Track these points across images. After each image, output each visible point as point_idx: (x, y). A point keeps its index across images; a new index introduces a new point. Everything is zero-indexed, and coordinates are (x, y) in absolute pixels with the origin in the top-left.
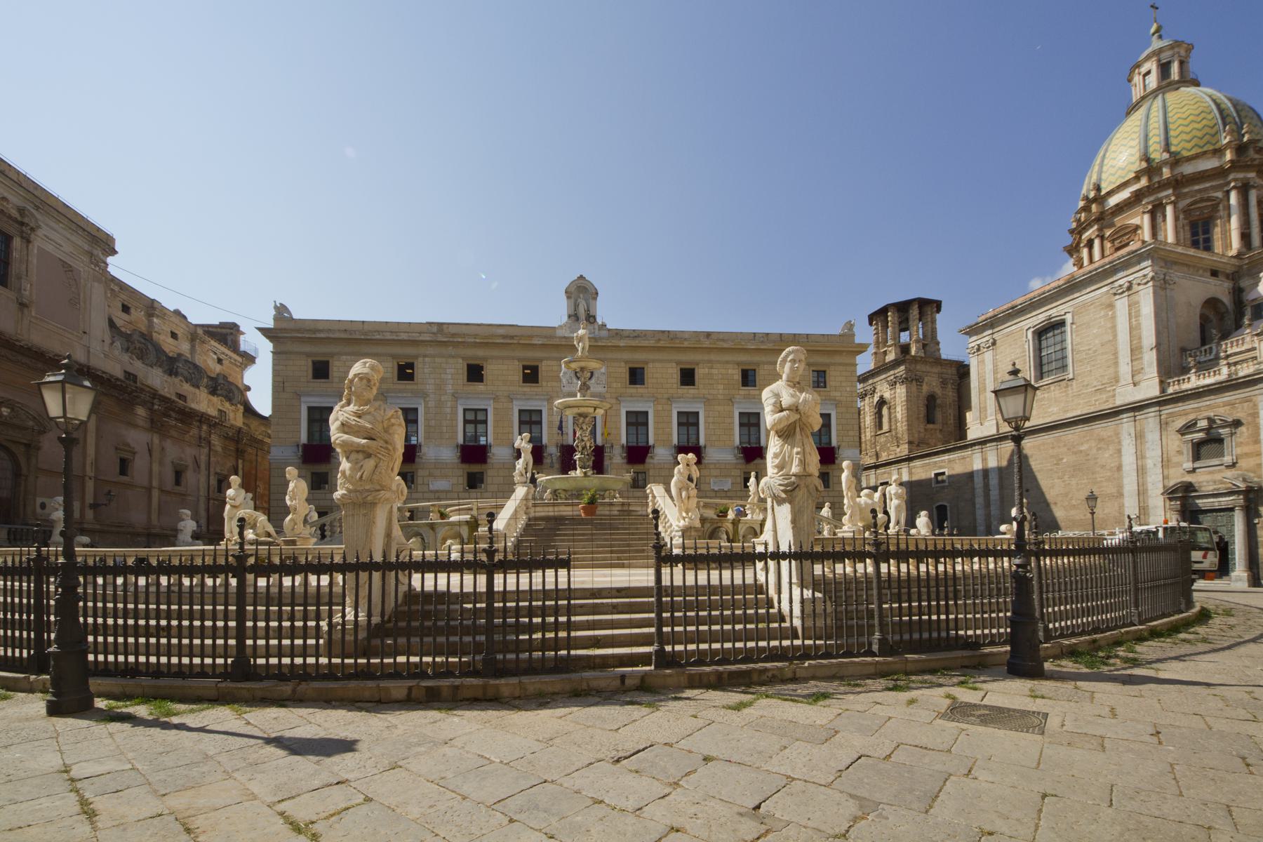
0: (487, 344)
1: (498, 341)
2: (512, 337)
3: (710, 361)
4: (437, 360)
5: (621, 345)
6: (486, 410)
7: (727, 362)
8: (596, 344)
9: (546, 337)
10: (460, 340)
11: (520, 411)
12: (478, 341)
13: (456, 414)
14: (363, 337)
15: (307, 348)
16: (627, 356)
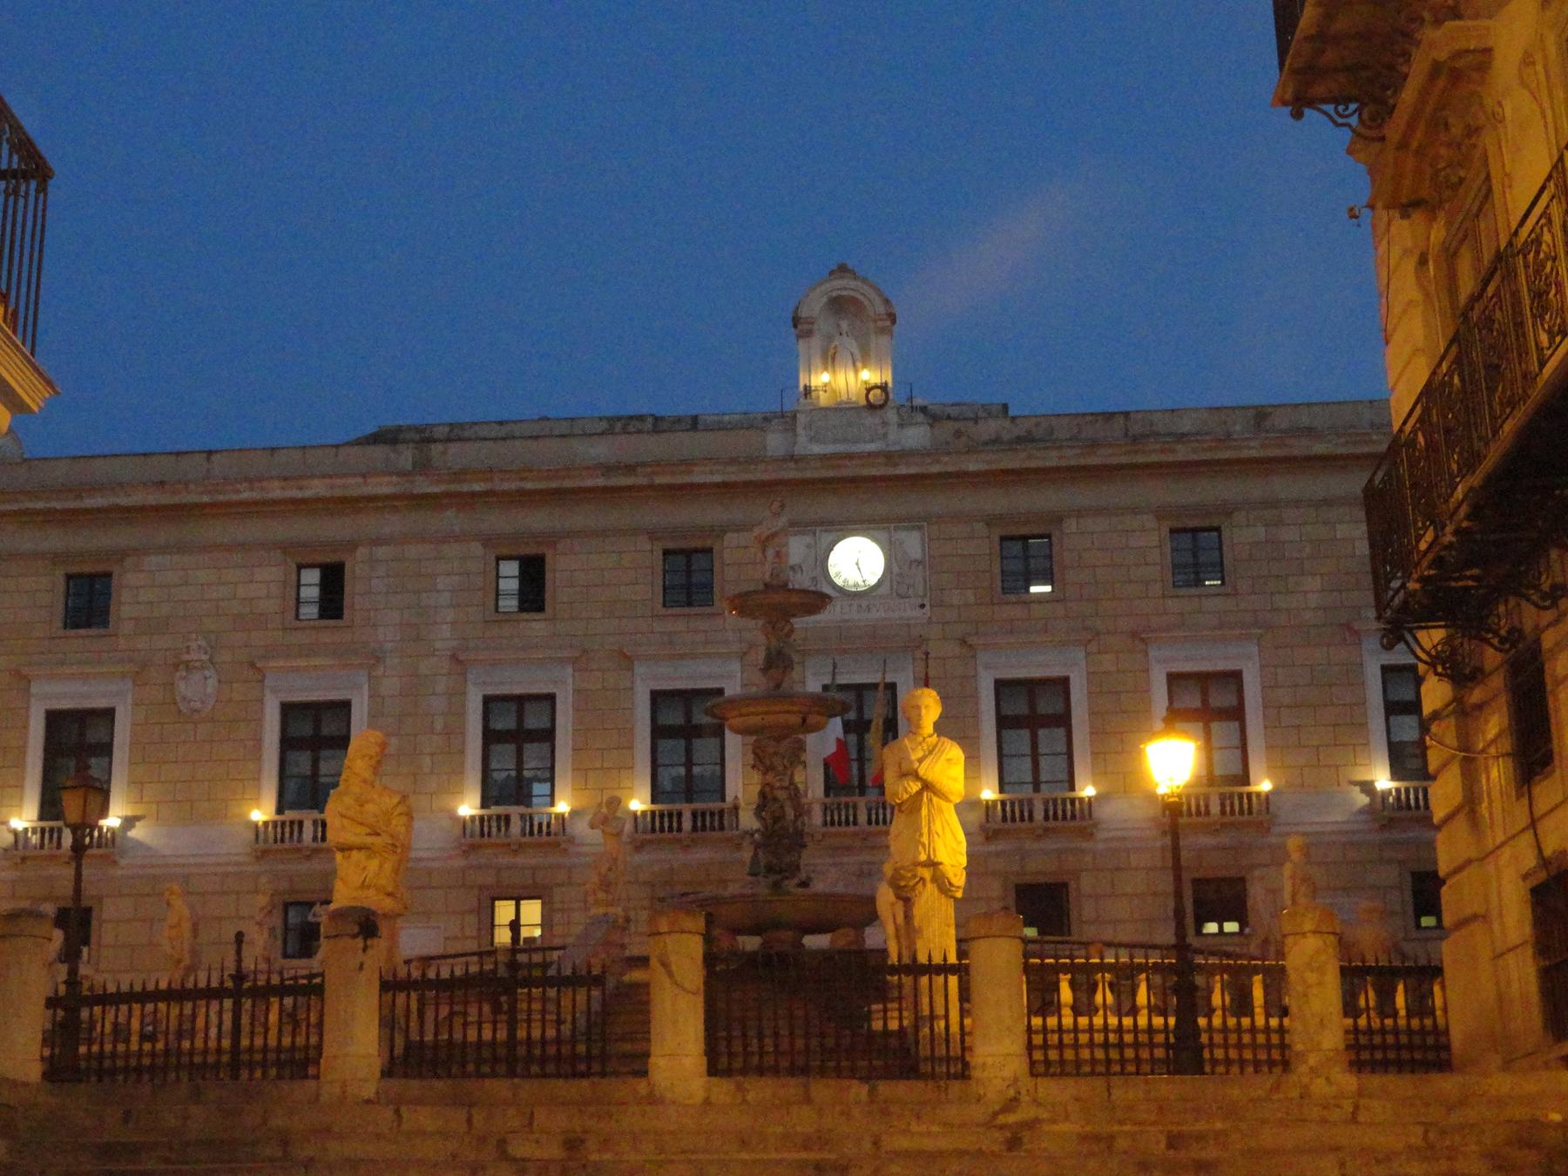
0: (558, 492)
1: (589, 483)
2: (630, 469)
3: (1273, 504)
4: (412, 551)
5: (972, 467)
6: (551, 698)
7: (1328, 502)
8: (891, 471)
9: (733, 461)
10: (477, 487)
11: (656, 696)
12: (529, 485)
13: (462, 713)
14: (206, 499)
15: (54, 540)
16: (997, 501)
